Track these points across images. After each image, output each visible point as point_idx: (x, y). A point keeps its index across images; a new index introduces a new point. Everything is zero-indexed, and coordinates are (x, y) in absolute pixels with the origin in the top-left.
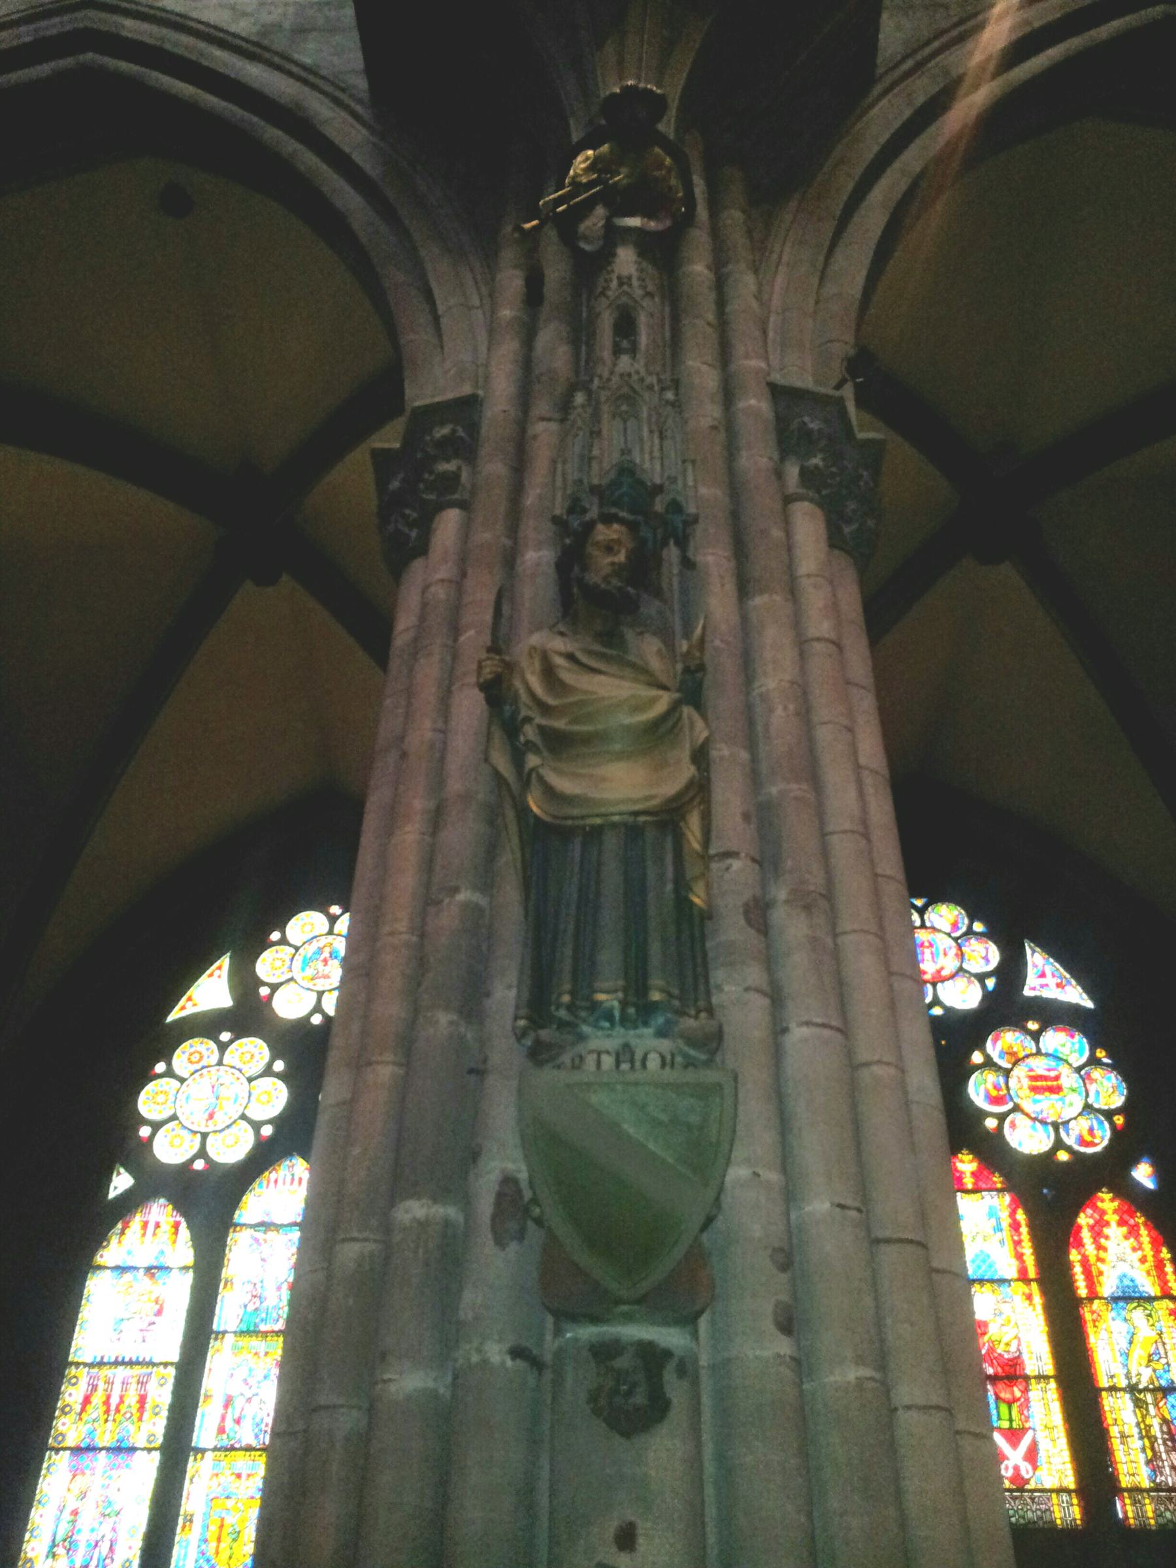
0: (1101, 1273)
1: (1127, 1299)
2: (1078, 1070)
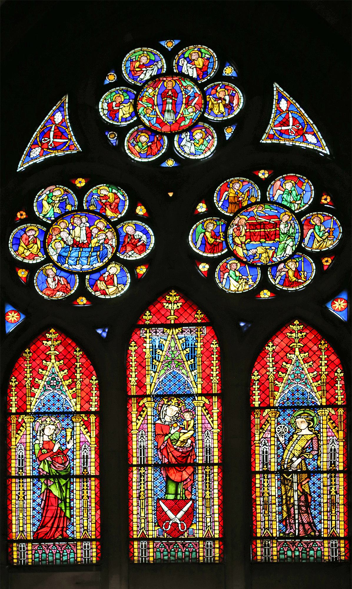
0: (277, 389)
1: (294, 408)
2: (299, 216)
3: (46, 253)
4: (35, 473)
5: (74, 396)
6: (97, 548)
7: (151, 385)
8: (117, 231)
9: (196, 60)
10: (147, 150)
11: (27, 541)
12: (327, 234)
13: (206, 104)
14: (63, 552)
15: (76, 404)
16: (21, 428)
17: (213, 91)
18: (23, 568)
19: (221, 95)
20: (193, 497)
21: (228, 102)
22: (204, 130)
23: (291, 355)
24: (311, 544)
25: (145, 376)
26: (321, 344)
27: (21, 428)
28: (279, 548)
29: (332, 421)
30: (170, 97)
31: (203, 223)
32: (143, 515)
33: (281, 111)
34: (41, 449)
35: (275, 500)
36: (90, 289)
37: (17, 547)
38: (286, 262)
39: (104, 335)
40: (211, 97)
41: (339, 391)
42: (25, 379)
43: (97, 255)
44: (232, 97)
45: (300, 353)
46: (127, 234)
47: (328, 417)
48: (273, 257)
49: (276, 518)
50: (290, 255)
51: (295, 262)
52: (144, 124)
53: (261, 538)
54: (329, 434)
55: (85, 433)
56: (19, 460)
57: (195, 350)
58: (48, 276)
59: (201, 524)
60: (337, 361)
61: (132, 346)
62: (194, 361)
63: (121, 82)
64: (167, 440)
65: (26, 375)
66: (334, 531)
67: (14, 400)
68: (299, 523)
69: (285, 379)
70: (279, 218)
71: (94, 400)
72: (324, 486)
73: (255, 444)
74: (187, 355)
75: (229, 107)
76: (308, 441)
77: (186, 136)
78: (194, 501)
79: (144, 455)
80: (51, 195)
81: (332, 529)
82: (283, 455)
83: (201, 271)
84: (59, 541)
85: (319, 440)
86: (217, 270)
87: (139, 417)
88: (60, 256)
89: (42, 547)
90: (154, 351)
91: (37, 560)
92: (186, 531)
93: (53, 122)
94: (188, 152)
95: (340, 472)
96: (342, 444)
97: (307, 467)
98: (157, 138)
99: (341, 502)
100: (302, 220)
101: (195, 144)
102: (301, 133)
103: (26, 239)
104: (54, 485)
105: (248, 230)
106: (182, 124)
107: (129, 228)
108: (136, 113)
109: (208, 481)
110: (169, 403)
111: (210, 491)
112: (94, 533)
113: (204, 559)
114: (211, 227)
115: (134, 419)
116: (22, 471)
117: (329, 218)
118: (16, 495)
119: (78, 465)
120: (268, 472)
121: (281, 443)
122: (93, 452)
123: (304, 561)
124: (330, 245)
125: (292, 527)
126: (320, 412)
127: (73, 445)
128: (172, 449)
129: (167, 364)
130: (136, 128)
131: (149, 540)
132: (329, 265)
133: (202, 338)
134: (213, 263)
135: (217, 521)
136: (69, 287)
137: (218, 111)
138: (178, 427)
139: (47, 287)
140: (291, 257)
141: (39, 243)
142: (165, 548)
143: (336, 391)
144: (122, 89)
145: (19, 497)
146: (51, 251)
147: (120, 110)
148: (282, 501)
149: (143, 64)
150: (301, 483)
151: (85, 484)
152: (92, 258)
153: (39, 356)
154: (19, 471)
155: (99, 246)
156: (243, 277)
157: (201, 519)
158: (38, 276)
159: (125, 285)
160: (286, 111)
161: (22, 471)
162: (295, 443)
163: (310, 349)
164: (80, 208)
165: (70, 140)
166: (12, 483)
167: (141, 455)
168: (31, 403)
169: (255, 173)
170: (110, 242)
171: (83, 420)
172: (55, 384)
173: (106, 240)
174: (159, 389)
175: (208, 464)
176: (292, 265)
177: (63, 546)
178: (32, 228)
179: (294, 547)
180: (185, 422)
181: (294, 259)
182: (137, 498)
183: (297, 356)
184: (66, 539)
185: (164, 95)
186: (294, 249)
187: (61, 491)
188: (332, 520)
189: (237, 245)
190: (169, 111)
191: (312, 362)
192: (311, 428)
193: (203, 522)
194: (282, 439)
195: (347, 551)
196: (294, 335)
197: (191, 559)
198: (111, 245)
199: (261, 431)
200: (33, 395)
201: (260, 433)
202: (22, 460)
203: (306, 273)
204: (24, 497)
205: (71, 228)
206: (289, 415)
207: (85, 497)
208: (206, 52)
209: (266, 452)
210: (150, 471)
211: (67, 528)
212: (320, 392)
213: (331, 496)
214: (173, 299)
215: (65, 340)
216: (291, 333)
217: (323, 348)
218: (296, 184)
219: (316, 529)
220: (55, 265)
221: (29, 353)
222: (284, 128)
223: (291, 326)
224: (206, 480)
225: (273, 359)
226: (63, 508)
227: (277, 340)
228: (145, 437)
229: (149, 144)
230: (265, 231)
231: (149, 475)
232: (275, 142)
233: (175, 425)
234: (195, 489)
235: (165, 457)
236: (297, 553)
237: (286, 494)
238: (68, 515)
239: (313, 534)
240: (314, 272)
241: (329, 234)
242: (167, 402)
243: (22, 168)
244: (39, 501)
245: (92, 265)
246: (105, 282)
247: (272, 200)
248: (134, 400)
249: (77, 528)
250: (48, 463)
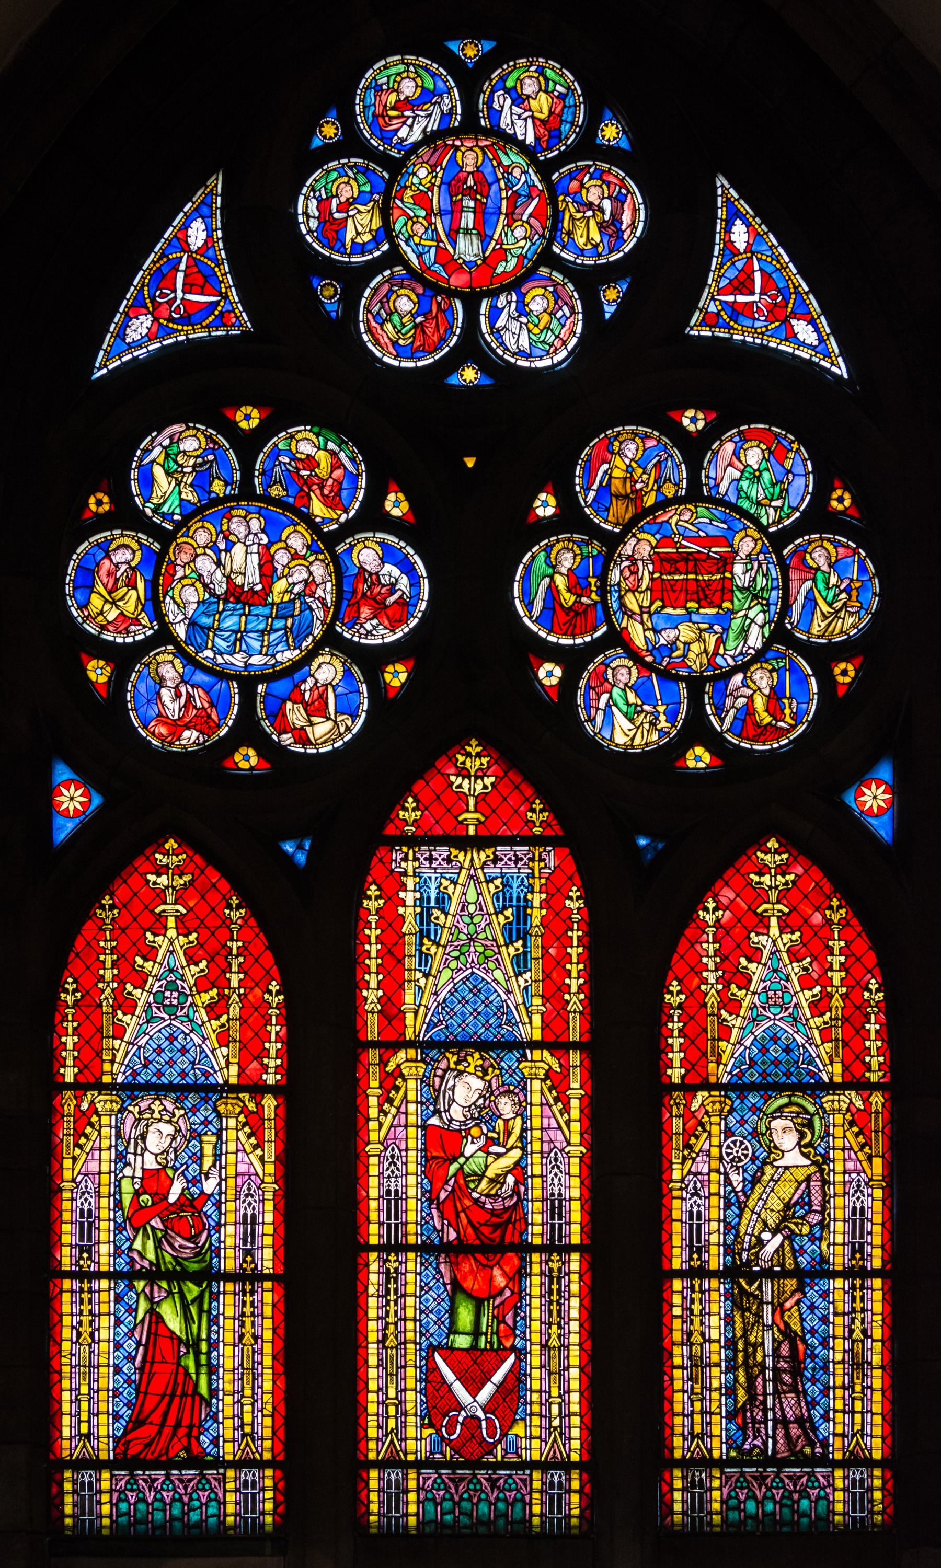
0: (725, 1033)
1: (768, 1088)
2: (777, 541)
3: (159, 615)
4: (122, 1263)
5: (224, 1039)
6: (275, 1489)
7: (416, 1013)
9: (533, 97)
10: (414, 337)
11: (98, 1465)
12: (844, 596)
13: (557, 217)
14: (191, 1499)
15: (228, 1063)
16: (88, 1130)
17: (574, 184)
18: (88, 1540)
19: (593, 196)
20: (519, 1343)
21: (608, 215)
22: (551, 289)
23: (761, 937)
24: (804, 1480)
25: (402, 987)
26: (830, 908)
27: (88, 1130)
28: (725, 1490)
29: (856, 1129)
30: (471, 192)
31: (548, 549)
32: (392, 1393)
33: (736, 252)
34: (137, 1194)
35: (717, 1353)
36: (266, 725)
37: (74, 1482)
38: (748, 669)
39: (301, 858)
40: (568, 199)
41: (873, 1045)
42: (100, 985)
43: (286, 627)
44: (618, 201)
45: (781, 932)
46: (362, 569)
47: (848, 1116)
48: (716, 653)
49: (720, 1406)
50: (757, 651)
51: (771, 671)
52: (406, 264)
53: (683, 1463)
54: (850, 1165)
55: (249, 1149)
56: (82, 1224)
57: (526, 915)
58: (161, 682)
59: (536, 1421)
60: (871, 959)
61: (369, 898)
62: (525, 946)
63: (351, 144)
64: (455, 1175)
65: (101, 972)
66: (858, 1443)
67: (70, 1046)
68: (775, 1420)
69: (745, 1004)
70: (731, 546)
71: (273, 1053)
72: (836, 1314)
73: (671, 1190)
74: (507, 929)
75: (612, 228)
76: (800, 1184)
77: (509, 303)
78: (521, 1354)
79: (396, 1218)
80: (175, 450)
81: (854, 1435)
82: (739, 1224)
83: (542, 685)
84: (181, 1466)
85: (825, 1182)
86: (582, 684)
87: (386, 1106)
88: (193, 624)
89: (136, 1482)
90: (424, 916)
91: (123, 1520)
92: (499, 1441)
93: (184, 246)
94: (514, 348)
95: (874, 1274)
96: (878, 1193)
97: (795, 1258)
98: (439, 304)
99: (877, 1360)
100: (785, 552)
101: (531, 326)
102: (781, 315)
103: (109, 574)
104: (169, 1300)
105: (656, 575)
106: (500, 270)
107: (367, 556)
108: (386, 232)
109: (555, 1297)
110: (461, 1068)
111: (559, 1327)
112: (268, 1444)
113: (542, 1522)
114: (567, 562)
115: (373, 1113)
116: (89, 1258)
117: (850, 552)
118: (73, 1327)
119: (230, 1242)
120: (702, 1272)
121: (734, 1188)
122: (269, 1206)
123: (785, 1529)
124: (849, 625)
125: (759, 1431)
126: (827, 1100)
127: (219, 1184)
128: (468, 1203)
129: (456, 954)
130: (387, 273)
131: (406, 1465)
132: (850, 684)
133: (543, 881)
134: (573, 661)
135: (575, 1414)
136: (214, 716)
137: (583, 240)
138: (483, 1138)
139: (160, 715)
140: (760, 656)
141: (141, 585)
142: (447, 1489)
143: (867, 1043)
144: (355, 165)
145: (79, 1335)
146: (170, 608)
147: (350, 221)
148: (735, 1357)
149: (407, 98)
150: (781, 1305)
151: (248, 1299)
152: (273, 636)
153: (135, 919)
154: (81, 1258)
155: (292, 601)
156: (646, 707)
157: (536, 1408)
158: (137, 683)
159: (354, 716)
160: (745, 252)
161: (89, 1258)
162: (768, 1190)
163: (806, 921)
164: (246, 492)
165: (226, 297)
166: (61, 1291)
167: (389, 1218)
168: (114, 1056)
169: (673, 414)
170: (320, 592)
171: (244, 1109)
172: (175, 1002)
174: (436, 1025)
175: (555, 1247)
176: (762, 679)
177: (190, 1480)
178: (126, 541)
179: (764, 1490)
180: (500, 1122)
181: (766, 662)
182: (378, 1342)
183: (773, 939)
184: (198, 1461)
185: (454, 185)
186: (767, 635)
187: (187, 1318)
188: (853, 1412)
189: (631, 615)
190: (467, 232)
191: (808, 959)
192: (806, 1146)
193: (541, 1416)
194: (736, 1178)
195: (889, 1499)
196: (766, 879)
197: (512, 1522)
198: (322, 600)
199: (686, 1153)
200: (119, 1032)
201: (684, 1159)
202: (90, 1224)
203: (795, 703)
204: (92, 1335)
205: (222, 546)
206: (754, 1109)
207: (248, 1339)
208: (557, 78)
209: (699, 1213)
210: (411, 1266)
211: (202, 1430)
212: (828, 1046)
213: (853, 1342)
214: (473, 765)
215: (202, 872)
216: (761, 874)
217: (836, 918)
218: (770, 453)
219: (817, 1437)
220: (181, 652)
221: (112, 907)
222: (741, 299)
223: (759, 854)
224: (551, 1292)
225: (717, 946)
226: (192, 1369)
228: (399, 1164)
229: (419, 320)
231: (410, 1277)
232: (721, 335)
233: (475, 1132)
234: (524, 1318)
235: (449, 1225)
236: (770, 1507)
237: (745, 1336)
238: (203, 1390)
239: (808, 1450)
240: (815, 702)
241: (850, 596)
242: (456, 1063)
243: (104, 371)
244: (130, 1345)
245: (273, 656)
246: (306, 706)
247: (713, 493)
248: (373, 1055)
249: (227, 1429)
250: (154, 1234)
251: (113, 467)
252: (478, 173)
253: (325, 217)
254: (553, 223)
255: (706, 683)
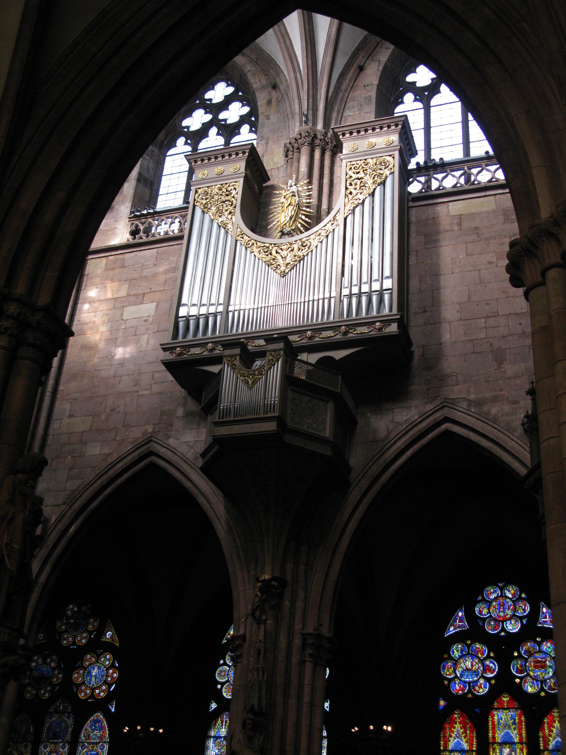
5: (467, 742)
8: (483, 665)
13: (515, 608)
30: (502, 606)
44: (525, 606)
52: (492, 617)
75: (524, 610)
88: (461, 674)
90: (499, 721)
93: (458, 616)
107: (487, 662)
108: (489, 612)
114: (519, 662)
146: (457, 672)
158: (452, 684)
164: (468, 653)
173: (479, 667)
176: (552, 681)
185: (499, 605)
189: (530, 670)
227: (548, 716)
230: (541, 665)
248: (491, 745)
251: (448, 650)
252: (503, 603)
253: (480, 611)
254: (515, 610)
255: (544, 682)
